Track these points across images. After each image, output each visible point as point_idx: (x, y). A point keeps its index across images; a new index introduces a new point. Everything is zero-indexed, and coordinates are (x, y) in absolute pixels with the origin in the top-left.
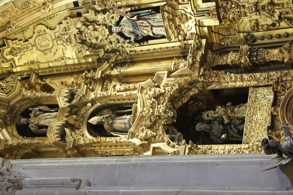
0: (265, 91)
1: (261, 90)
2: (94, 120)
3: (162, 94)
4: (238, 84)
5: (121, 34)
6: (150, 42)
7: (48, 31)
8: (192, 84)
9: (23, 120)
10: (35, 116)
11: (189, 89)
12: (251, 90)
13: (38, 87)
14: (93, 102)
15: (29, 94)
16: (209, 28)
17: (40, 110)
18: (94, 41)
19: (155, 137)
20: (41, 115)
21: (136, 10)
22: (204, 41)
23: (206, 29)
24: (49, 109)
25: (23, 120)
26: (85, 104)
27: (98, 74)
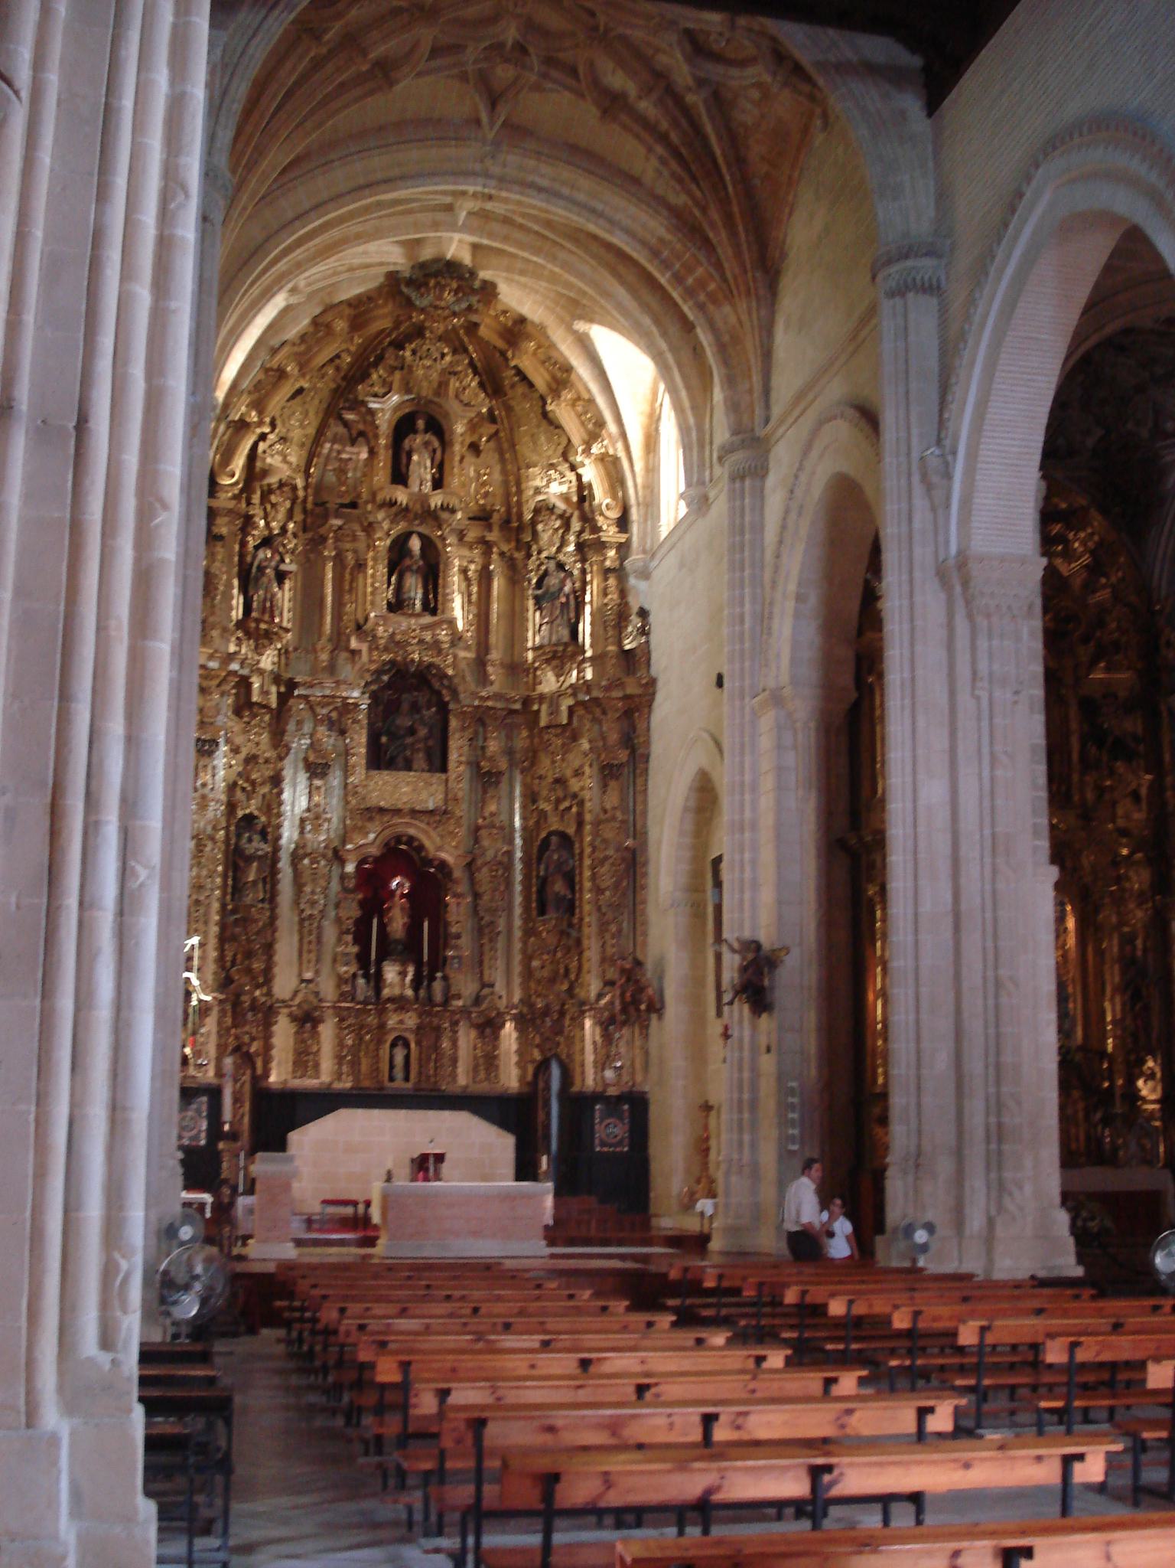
0: (440, 796)
1: (442, 788)
2: (415, 544)
3: (440, 652)
4: (453, 756)
5: (546, 573)
6: (538, 614)
7: (561, 449)
8: (454, 693)
9: (421, 424)
10: (426, 444)
11: (449, 688)
12: (443, 776)
13: (475, 438)
14: (443, 538)
15: (460, 428)
16: (538, 711)
17: (434, 451)
18: (540, 527)
19: (377, 648)
20: (426, 456)
21: (576, 598)
22: (517, 706)
23: (536, 707)
24: (437, 462)
25: (421, 424)
26: (440, 528)
27: (493, 536)
